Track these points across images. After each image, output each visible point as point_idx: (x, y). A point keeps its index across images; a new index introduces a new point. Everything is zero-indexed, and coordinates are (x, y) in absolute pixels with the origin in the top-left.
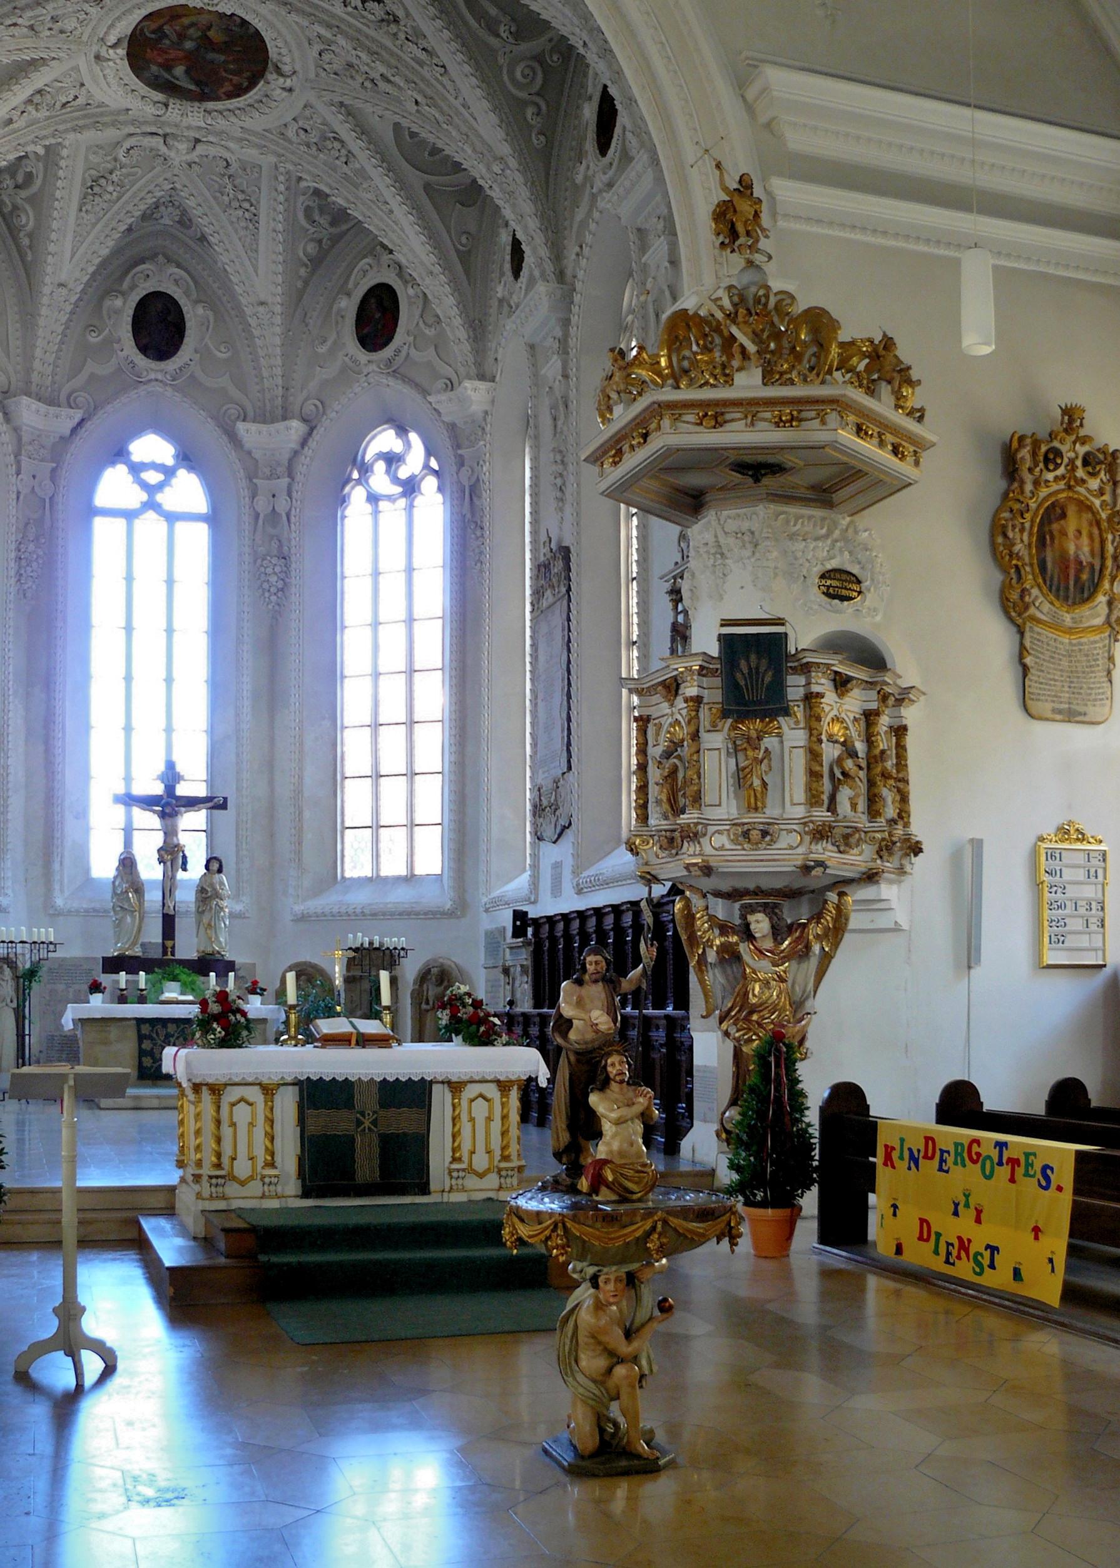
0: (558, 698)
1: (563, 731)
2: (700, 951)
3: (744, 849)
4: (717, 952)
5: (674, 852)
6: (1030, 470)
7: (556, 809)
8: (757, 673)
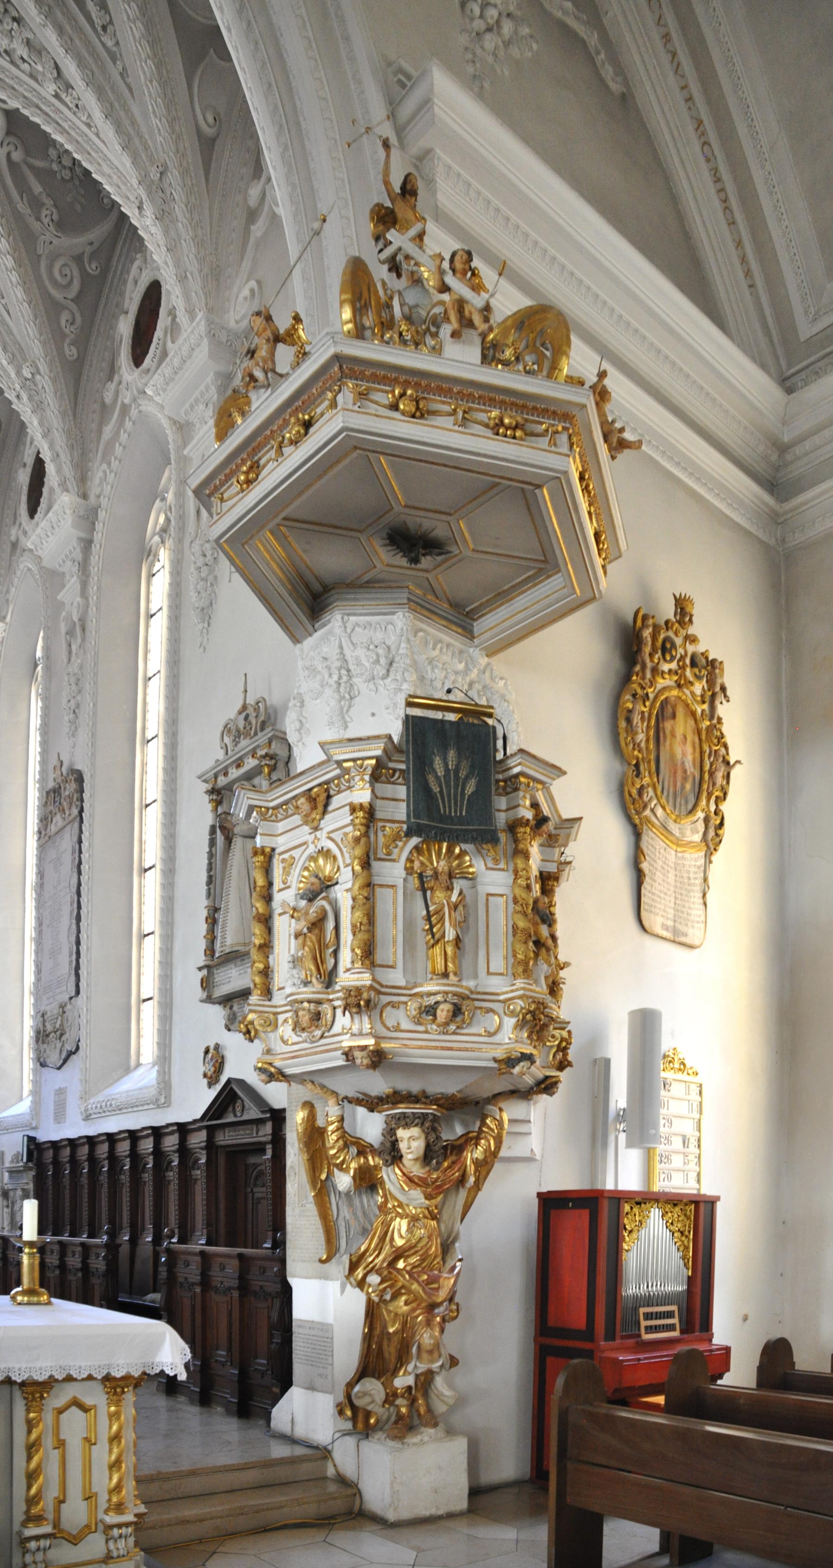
0: (66, 921)
1: (71, 955)
2: (323, 1177)
3: (426, 1032)
4: (354, 1178)
5: (318, 1033)
6: (651, 655)
7: (62, 1035)
8: (457, 777)
